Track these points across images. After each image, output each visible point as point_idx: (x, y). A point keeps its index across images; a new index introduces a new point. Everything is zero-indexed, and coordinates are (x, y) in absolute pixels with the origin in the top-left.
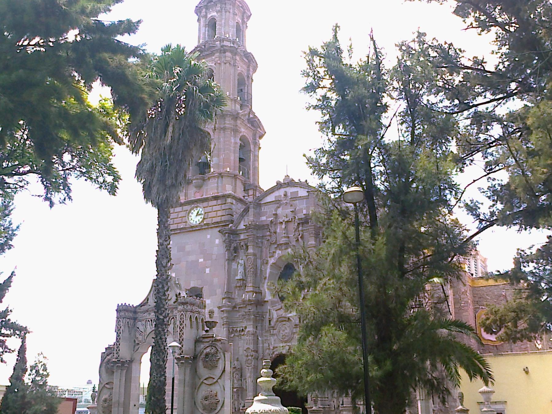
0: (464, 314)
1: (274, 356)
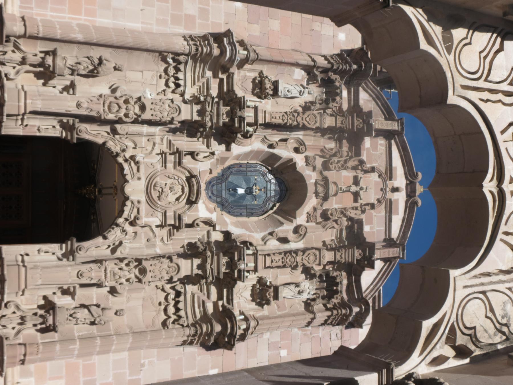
1: (120, 160)
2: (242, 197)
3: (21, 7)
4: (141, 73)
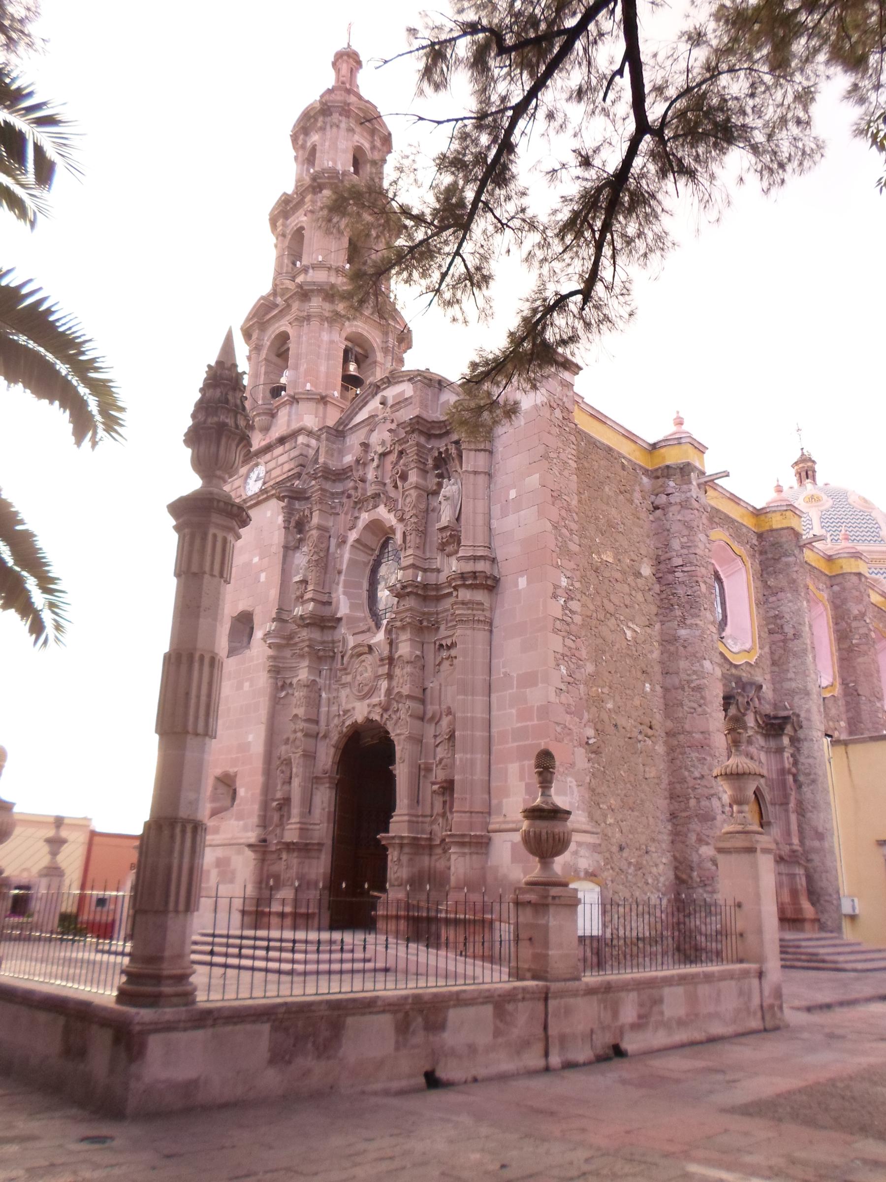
0: (860, 660)
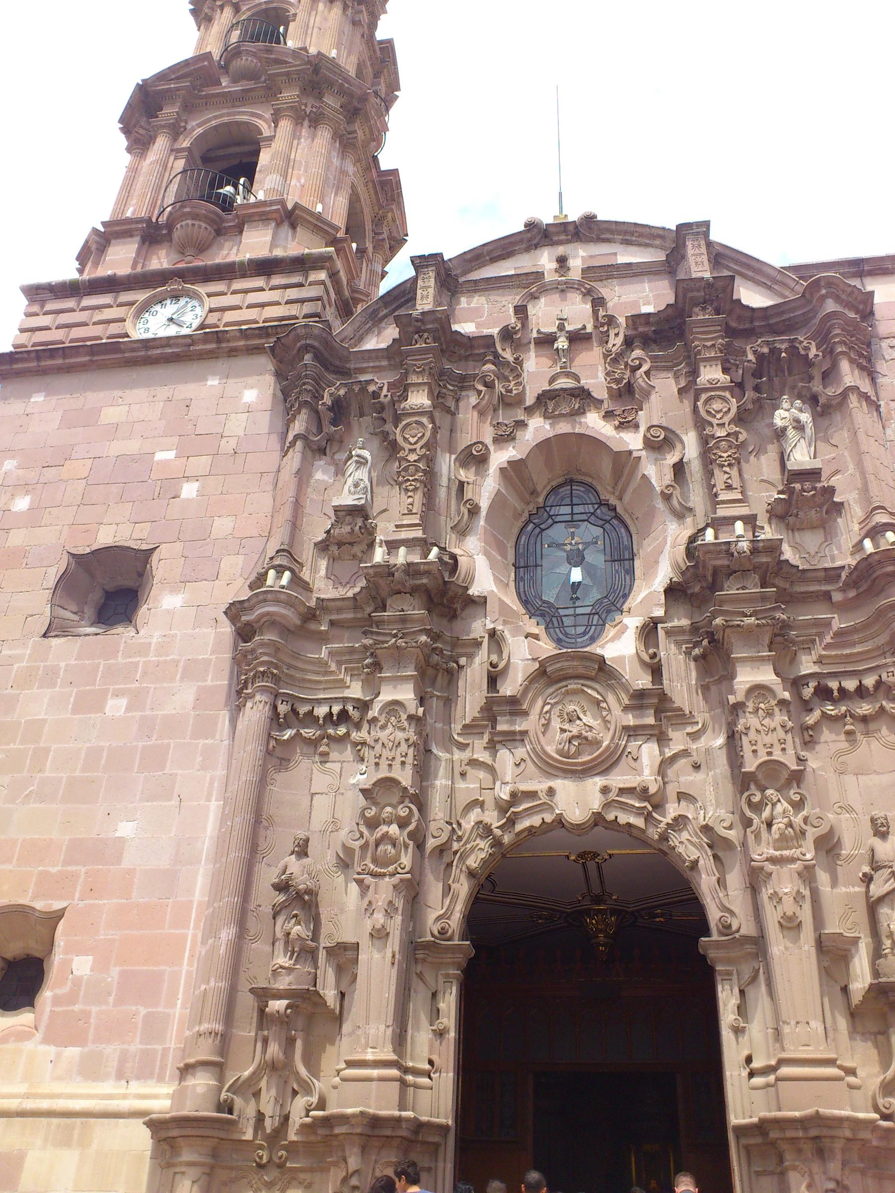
2: (589, 571)
3: (161, 1079)
4: (316, 797)
